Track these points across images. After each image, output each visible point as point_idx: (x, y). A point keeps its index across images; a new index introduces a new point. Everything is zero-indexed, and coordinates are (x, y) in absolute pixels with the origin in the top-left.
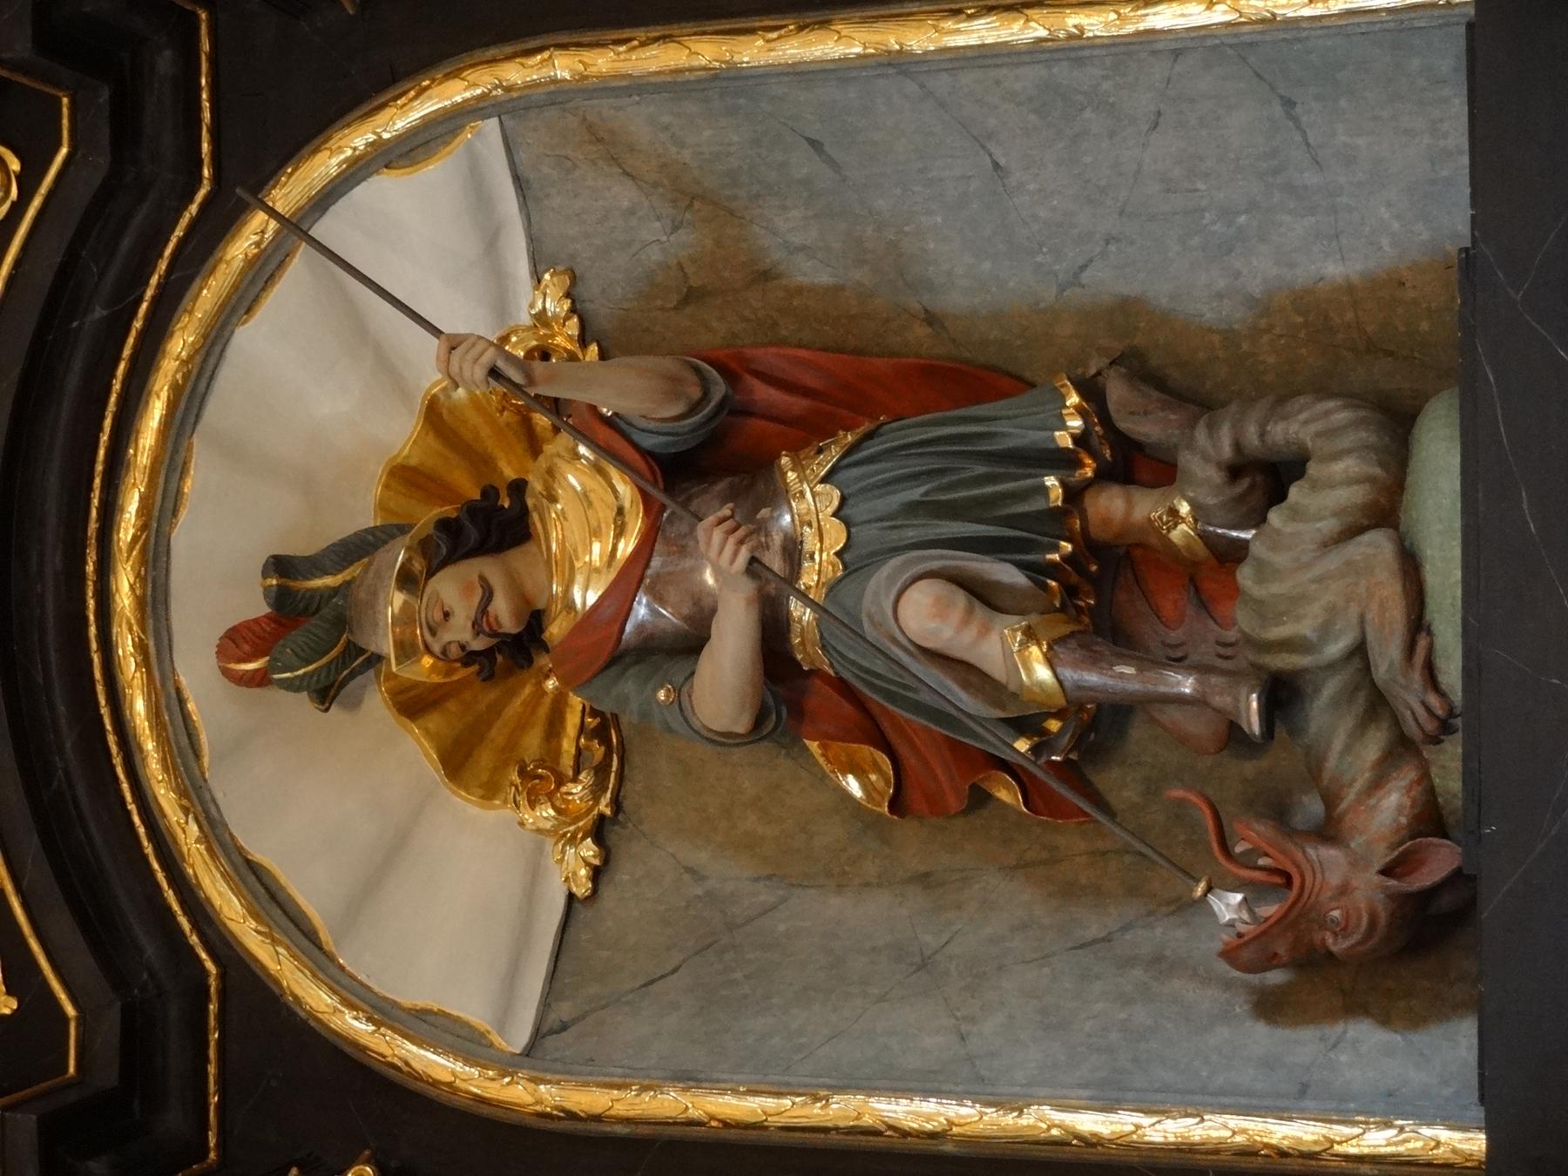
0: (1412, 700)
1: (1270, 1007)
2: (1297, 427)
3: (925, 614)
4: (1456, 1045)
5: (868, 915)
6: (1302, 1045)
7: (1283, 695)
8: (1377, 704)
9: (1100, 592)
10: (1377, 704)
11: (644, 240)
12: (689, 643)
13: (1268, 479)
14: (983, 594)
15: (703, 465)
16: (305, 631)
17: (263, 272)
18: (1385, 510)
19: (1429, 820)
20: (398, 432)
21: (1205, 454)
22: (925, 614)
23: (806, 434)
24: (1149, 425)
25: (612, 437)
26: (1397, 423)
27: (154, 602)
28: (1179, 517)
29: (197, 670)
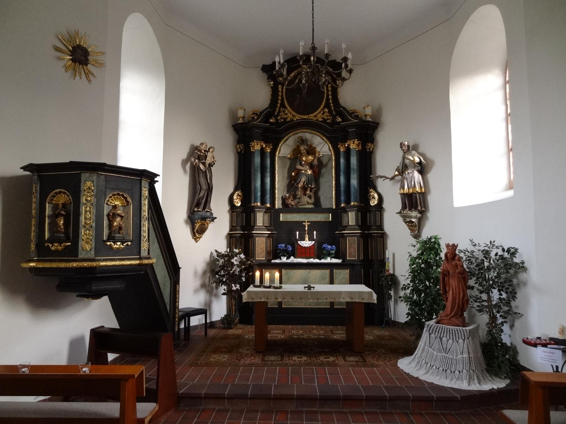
0: (298, 205)
1: (282, 197)
2: (313, 200)
3: (303, 179)
4: (281, 207)
5: (286, 175)
6: (281, 199)
7: (299, 198)
8: (298, 203)
9: (304, 189)
10: (298, 203)
11: (325, 161)
12: (301, 165)
13: (310, 197)
14: (304, 183)
15: (311, 166)
16: (303, 141)
17: (323, 140)
18: (308, 203)
19: (292, 205)
20: (314, 146)
21: (312, 194)
22: (303, 179)
23: (313, 172)
24: (313, 191)
25: (313, 161)
26: (313, 204)
27: (304, 132)
28: (308, 192)
29: (300, 135)
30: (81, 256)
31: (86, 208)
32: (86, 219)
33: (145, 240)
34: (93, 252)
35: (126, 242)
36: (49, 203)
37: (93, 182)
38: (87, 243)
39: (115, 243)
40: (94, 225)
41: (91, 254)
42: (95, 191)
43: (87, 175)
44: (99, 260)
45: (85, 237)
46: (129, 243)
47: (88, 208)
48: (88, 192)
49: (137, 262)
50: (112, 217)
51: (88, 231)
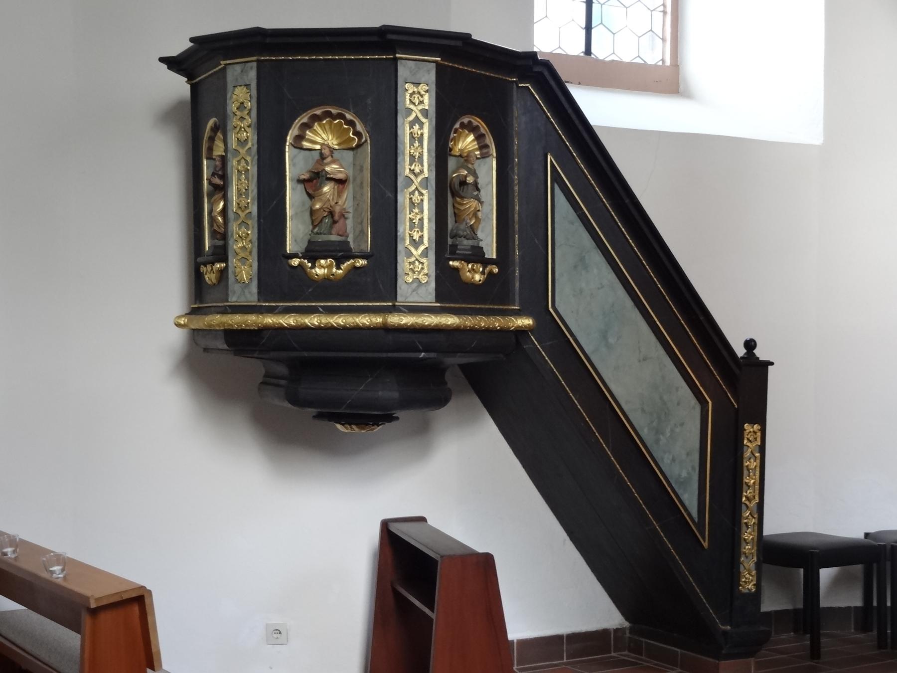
30: (233, 300)
31: (239, 161)
32: (240, 194)
33: (416, 253)
34: (254, 288)
35: (348, 258)
36: (207, 159)
37: (247, 86)
38: (244, 260)
39: (313, 259)
40: (254, 209)
41: (250, 293)
42: (254, 113)
43: (238, 68)
44: (271, 311)
45: (240, 245)
46: (361, 262)
47: (243, 163)
48: (242, 119)
49: (378, 320)
50: (313, 180)
51: (243, 229)
